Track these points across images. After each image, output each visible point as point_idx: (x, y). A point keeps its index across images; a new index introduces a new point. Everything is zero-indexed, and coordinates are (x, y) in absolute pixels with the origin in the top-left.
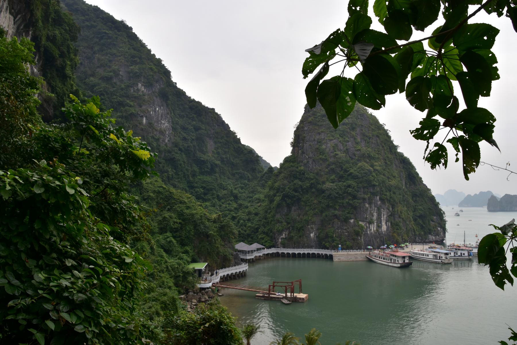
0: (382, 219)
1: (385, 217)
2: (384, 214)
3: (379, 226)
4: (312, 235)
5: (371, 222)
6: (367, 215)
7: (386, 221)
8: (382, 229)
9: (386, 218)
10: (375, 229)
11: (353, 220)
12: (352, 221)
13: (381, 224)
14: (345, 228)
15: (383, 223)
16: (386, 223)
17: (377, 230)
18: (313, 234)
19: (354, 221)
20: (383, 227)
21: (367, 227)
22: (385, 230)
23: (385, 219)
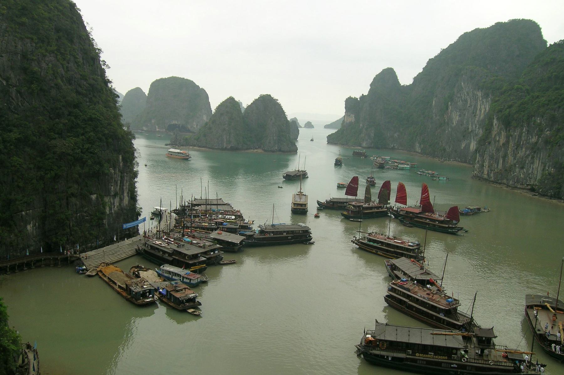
0: (125, 187)
1: (128, 184)
2: (126, 181)
3: (121, 200)
4: (29, 227)
5: (115, 196)
6: (112, 186)
7: (128, 190)
8: (124, 201)
9: (129, 186)
10: (118, 204)
11: (95, 195)
12: (94, 197)
13: (123, 196)
14: (85, 210)
15: (125, 194)
16: (128, 193)
17: (120, 204)
18: (31, 225)
19: (97, 197)
20: (124, 200)
21: (111, 202)
22: (127, 203)
23: (128, 187)
